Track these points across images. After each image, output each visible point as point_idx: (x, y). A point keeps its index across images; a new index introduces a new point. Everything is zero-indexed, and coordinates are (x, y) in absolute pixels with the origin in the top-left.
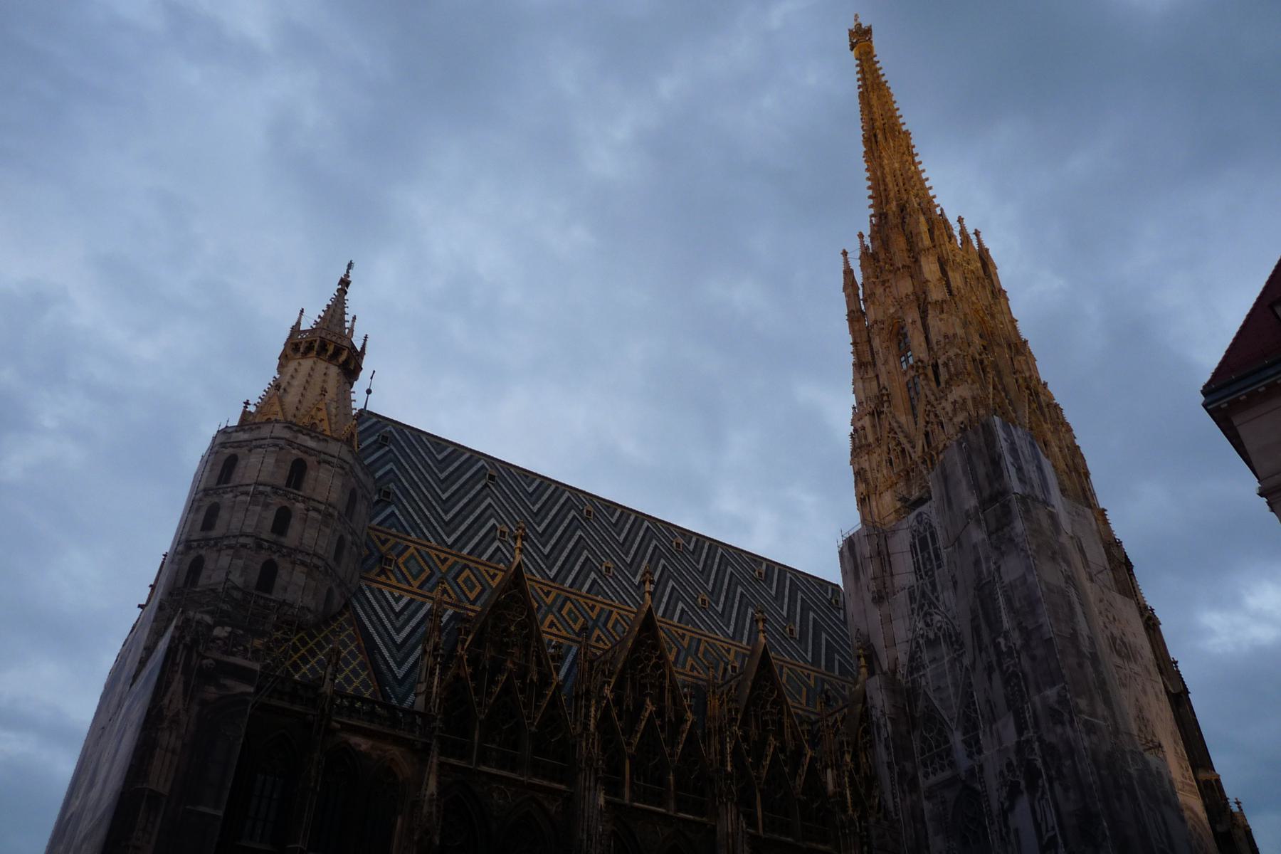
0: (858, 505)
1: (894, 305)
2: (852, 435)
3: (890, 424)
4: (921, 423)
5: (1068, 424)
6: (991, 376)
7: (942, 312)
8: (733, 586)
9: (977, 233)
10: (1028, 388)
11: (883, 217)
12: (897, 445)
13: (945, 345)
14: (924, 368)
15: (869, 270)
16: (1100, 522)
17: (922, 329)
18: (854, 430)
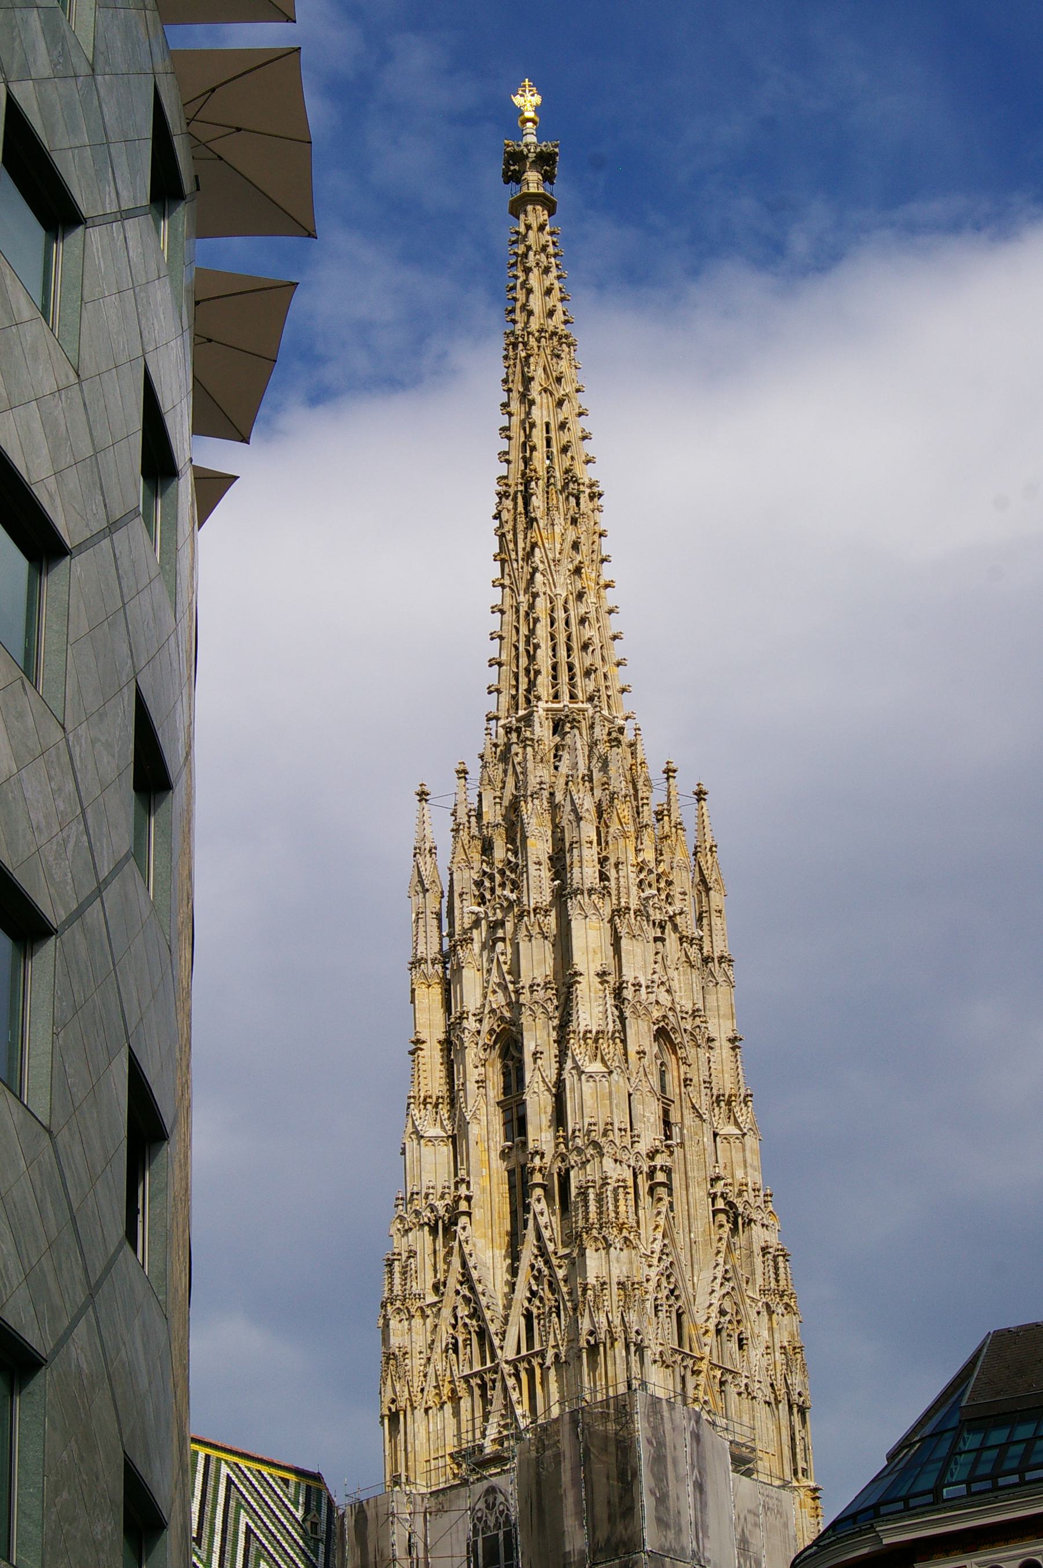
3: (464, 1264)
4: (521, 1293)
6: (664, 1209)
9: (700, 795)
12: (470, 1316)
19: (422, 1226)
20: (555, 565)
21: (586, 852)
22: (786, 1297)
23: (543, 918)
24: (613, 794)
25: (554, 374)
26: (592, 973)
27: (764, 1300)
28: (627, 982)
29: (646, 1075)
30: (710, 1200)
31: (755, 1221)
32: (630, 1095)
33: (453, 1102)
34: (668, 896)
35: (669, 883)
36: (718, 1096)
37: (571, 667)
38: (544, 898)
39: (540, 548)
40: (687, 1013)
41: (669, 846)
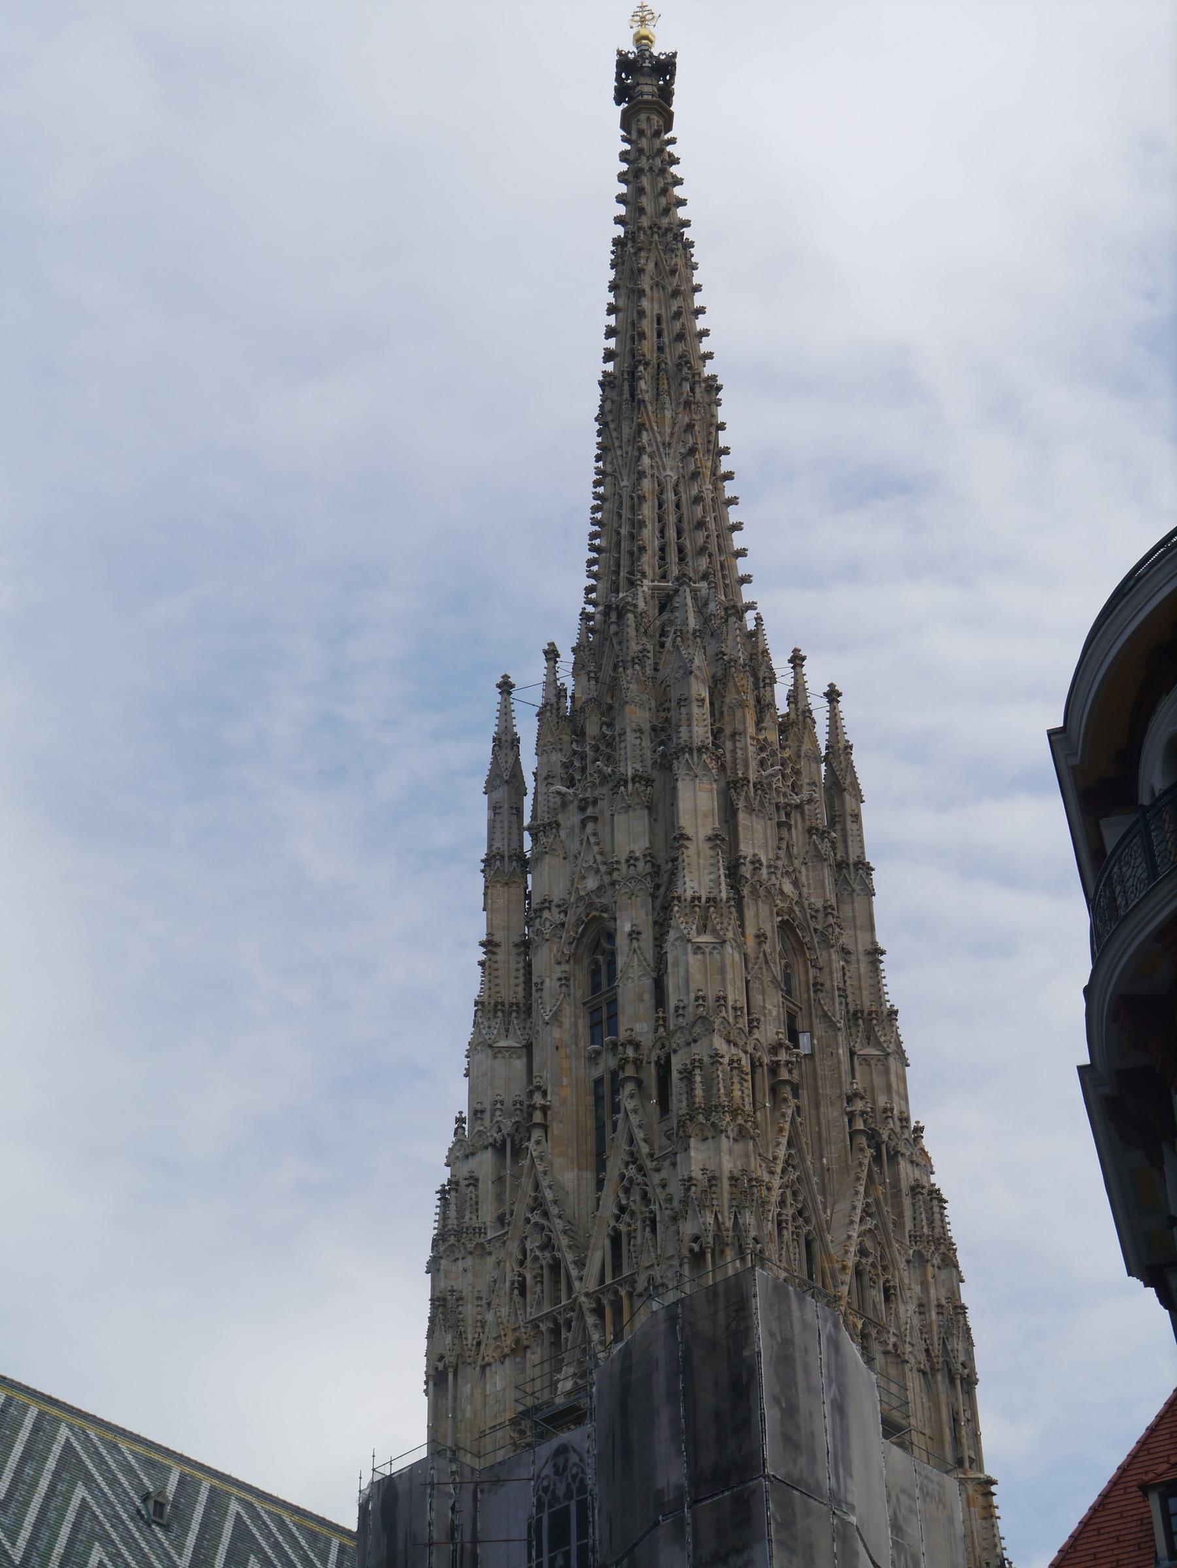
0: (426, 1383)
1: (597, 871)
2: (442, 1191)
3: (537, 1187)
4: (609, 1208)
5: (950, 1247)
6: (790, 1112)
7: (702, 929)
8: (79, 1548)
9: (832, 695)
10: (873, 1136)
11: (613, 617)
13: (694, 1024)
14: (638, 1064)
15: (557, 758)
16: (976, 1511)
17: (649, 954)
18: (450, 1183)
19: (486, 1148)
20: (664, 448)
21: (695, 710)
22: (942, 1247)
23: (643, 788)
24: (729, 663)
25: (667, 268)
26: (702, 837)
27: (915, 1248)
28: (745, 858)
29: (767, 962)
30: (846, 1120)
31: (902, 1155)
32: (747, 982)
33: (529, 1011)
34: (794, 785)
35: (798, 773)
36: (855, 1013)
37: (681, 550)
38: (645, 769)
39: (647, 431)
40: (817, 911)
41: (795, 734)
